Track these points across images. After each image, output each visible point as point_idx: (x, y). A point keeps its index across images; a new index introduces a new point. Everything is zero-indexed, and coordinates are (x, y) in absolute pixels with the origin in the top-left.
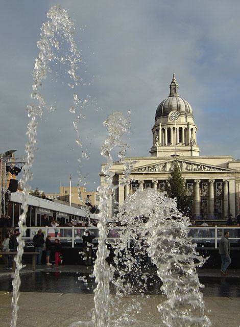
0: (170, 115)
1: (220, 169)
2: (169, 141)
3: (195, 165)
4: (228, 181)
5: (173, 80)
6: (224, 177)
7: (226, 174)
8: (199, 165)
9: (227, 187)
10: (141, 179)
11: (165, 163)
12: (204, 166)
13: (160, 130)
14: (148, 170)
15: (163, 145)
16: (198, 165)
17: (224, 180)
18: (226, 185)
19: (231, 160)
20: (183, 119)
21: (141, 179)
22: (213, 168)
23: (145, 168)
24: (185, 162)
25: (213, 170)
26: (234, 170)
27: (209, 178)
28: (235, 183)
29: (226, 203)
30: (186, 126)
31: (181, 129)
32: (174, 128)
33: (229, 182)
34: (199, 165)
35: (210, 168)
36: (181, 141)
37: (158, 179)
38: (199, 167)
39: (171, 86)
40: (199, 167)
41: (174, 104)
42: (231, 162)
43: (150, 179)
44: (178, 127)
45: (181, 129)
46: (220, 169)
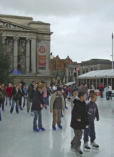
4: (30, 39)
6: (28, 36)
7: (28, 34)
9: (28, 45)
12: (10, 24)
16: (4, 23)
17: (27, 39)
18: (28, 43)
22: (18, 27)
25: (17, 29)
26: (37, 30)
27: (14, 36)
28: (36, 42)
29: (28, 59)
33: (30, 41)
35: (15, 26)
38: (5, 24)
40: (5, 24)
46: (24, 28)
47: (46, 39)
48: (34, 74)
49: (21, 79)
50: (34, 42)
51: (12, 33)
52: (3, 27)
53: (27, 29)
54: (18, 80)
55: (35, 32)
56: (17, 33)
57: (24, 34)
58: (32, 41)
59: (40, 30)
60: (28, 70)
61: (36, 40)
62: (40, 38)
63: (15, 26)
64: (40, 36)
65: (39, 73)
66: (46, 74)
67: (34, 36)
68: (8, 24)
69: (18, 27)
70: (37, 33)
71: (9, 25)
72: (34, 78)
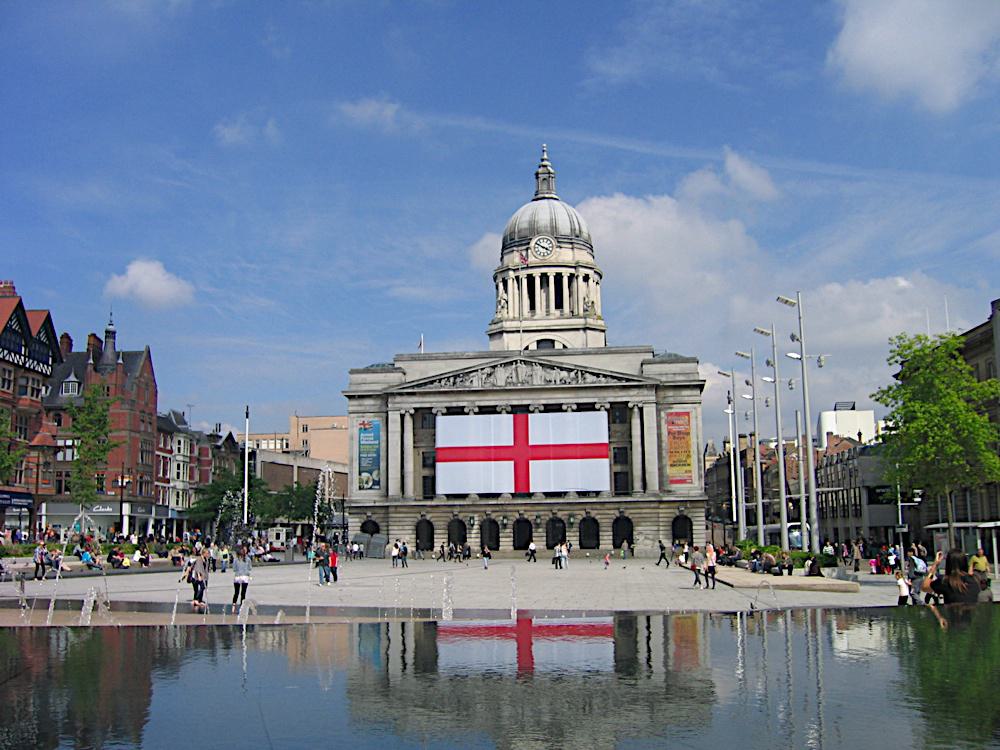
1: (620, 379)
2: (532, 307)
3: (562, 369)
4: (640, 405)
5: (543, 160)
6: (632, 397)
8: (572, 370)
9: (636, 422)
10: (439, 405)
11: (494, 367)
12: (584, 371)
13: (510, 282)
14: (454, 383)
19: (649, 356)
20: (566, 255)
21: (439, 405)
22: (605, 376)
23: (448, 378)
24: (541, 364)
25: (603, 382)
26: (657, 380)
27: (596, 400)
30: (573, 271)
31: (558, 278)
32: (544, 277)
33: (641, 410)
34: (572, 370)
35: (598, 375)
36: (559, 305)
37: (478, 403)
38: (573, 374)
39: (537, 174)
41: (543, 220)
42: (649, 363)
43: (461, 404)
44: (551, 272)
45: (558, 278)
46: (620, 379)
47: (686, 399)
48: (655, 495)
49: (618, 509)
50: (650, 412)
51: (590, 394)
52: (568, 381)
53: (628, 380)
54: (612, 512)
55: (652, 386)
56: (604, 393)
57: (621, 393)
58: (645, 409)
59: (664, 379)
60: (638, 485)
61: (654, 405)
62: (671, 400)
63: (598, 375)
64: (671, 393)
65: (670, 491)
66: (693, 493)
67: (651, 396)
68: (579, 373)
69: (605, 376)
70: (657, 388)
71: (582, 374)
72: (656, 505)
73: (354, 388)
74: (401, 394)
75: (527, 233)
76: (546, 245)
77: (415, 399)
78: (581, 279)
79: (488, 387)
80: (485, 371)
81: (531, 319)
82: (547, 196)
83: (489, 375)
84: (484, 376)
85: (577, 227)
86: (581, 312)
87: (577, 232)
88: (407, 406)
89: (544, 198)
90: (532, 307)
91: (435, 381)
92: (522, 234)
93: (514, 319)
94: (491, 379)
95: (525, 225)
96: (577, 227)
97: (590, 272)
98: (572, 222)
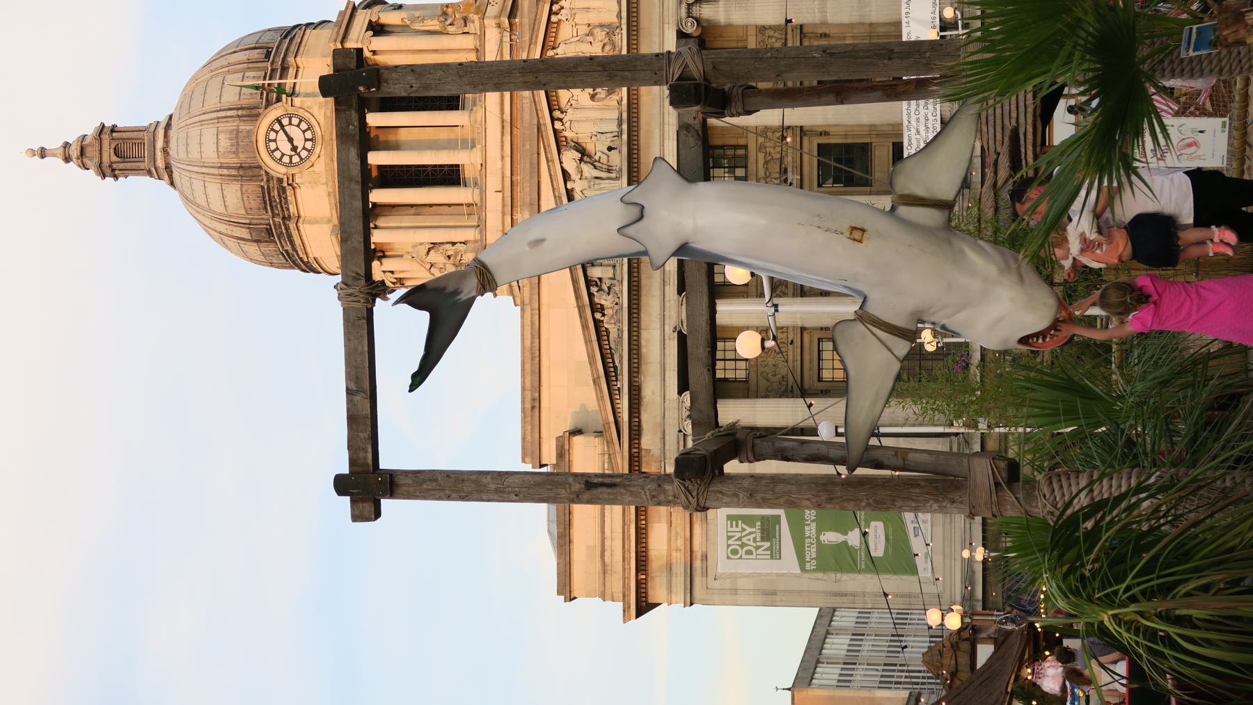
0: (278, 170)
2: (449, 176)
15: (475, 210)
73: (616, 585)
74: (636, 433)
75: (253, 188)
76: (299, 142)
77: (650, 389)
78: (380, 43)
79: (618, 160)
80: (571, 167)
81: (480, 184)
82: (160, 144)
83: (582, 151)
84: (588, 170)
85: (242, 56)
86: (469, 42)
87: (256, 54)
88: (672, 416)
89: (165, 151)
90: (449, 176)
91: (597, 324)
92: (255, 203)
93: (481, 226)
94: (597, 147)
95: (233, 192)
96: (242, 56)
97: (362, 19)
98: (230, 68)
